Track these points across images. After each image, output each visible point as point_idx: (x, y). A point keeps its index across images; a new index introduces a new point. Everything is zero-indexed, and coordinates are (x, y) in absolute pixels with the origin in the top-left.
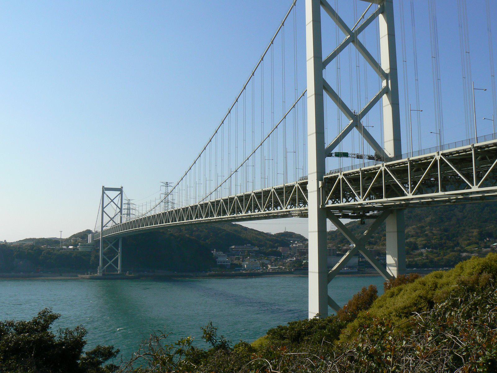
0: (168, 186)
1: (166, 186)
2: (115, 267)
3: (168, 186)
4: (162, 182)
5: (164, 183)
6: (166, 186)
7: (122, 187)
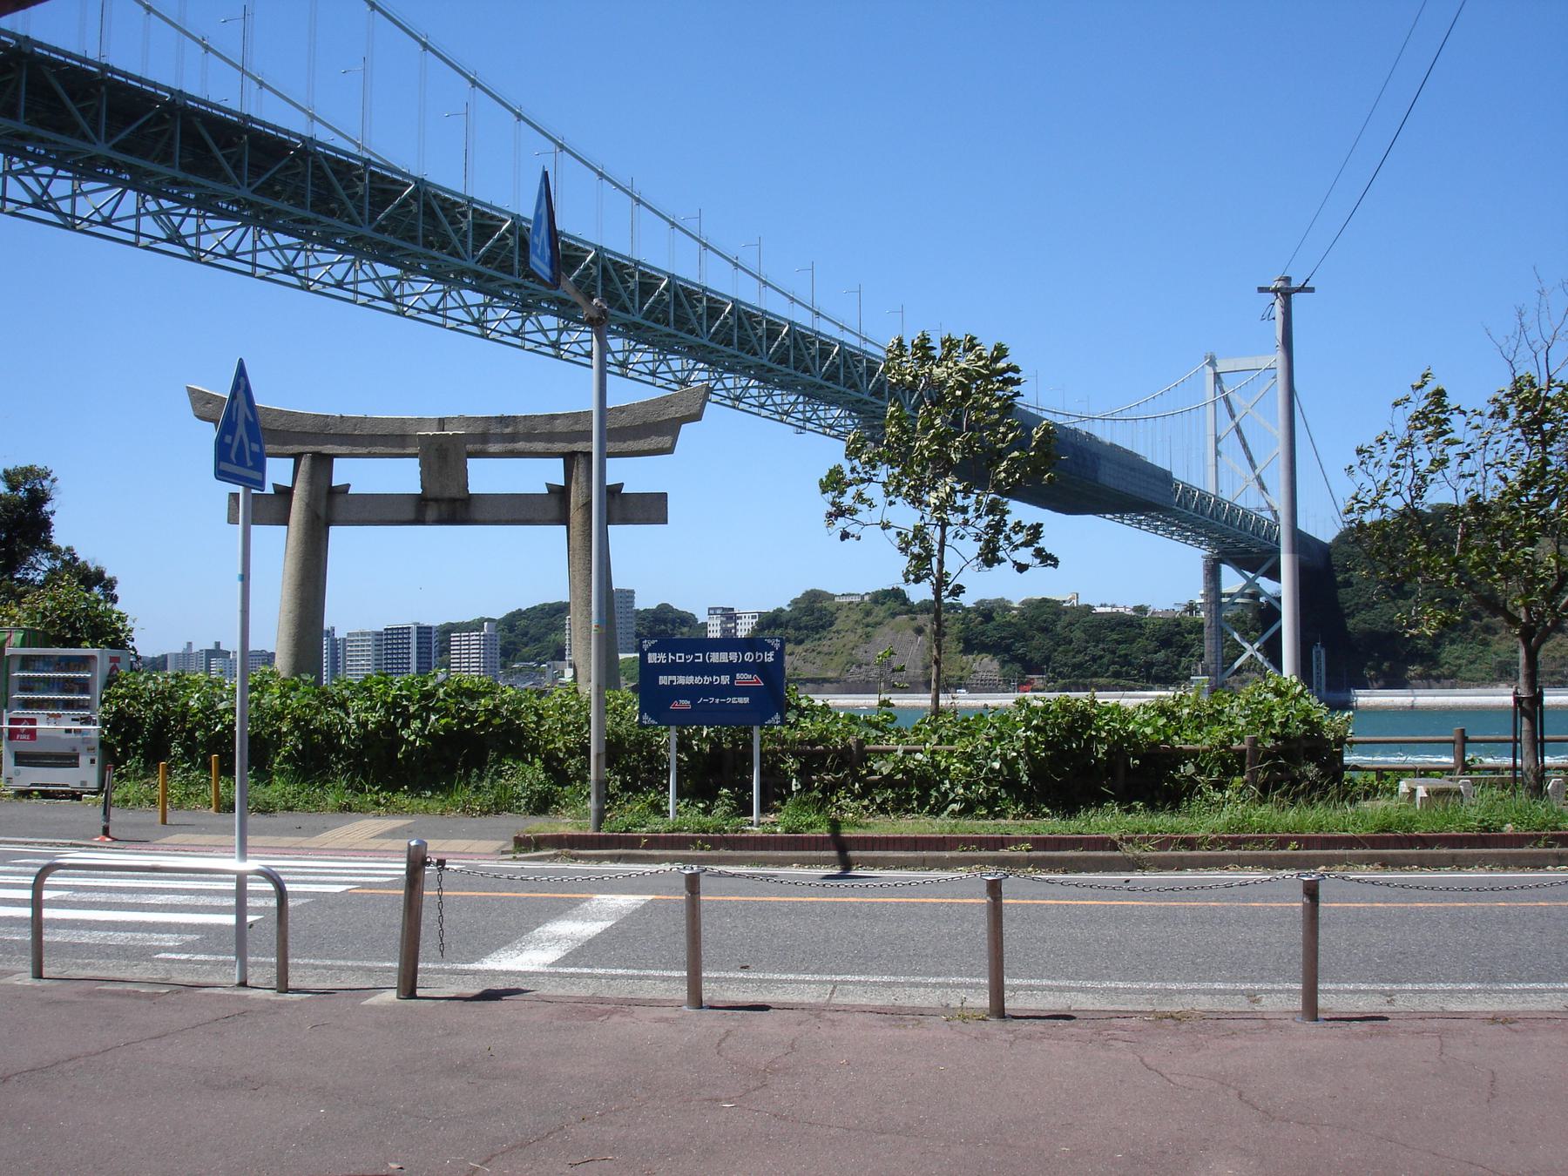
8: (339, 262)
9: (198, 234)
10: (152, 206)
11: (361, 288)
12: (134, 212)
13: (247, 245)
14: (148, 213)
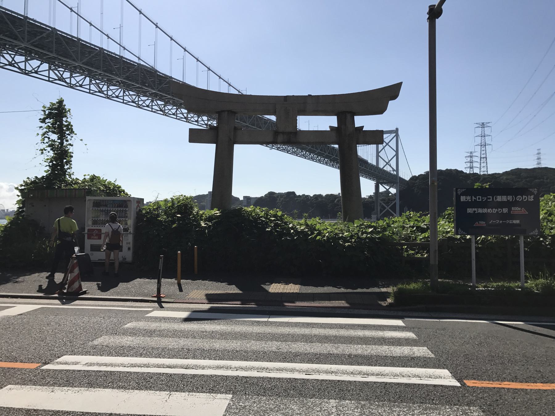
0: (485, 126)
3: (484, 127)
4: (477, 124)
5: (480, 124)
6: (482, 127)
7: (397, 129)
8: (148, 99)
9: (107, 90)
10: (94, 82)
11: (153, 107)
12: (89, 83)
13: (121, 94)
14: (93, 84)
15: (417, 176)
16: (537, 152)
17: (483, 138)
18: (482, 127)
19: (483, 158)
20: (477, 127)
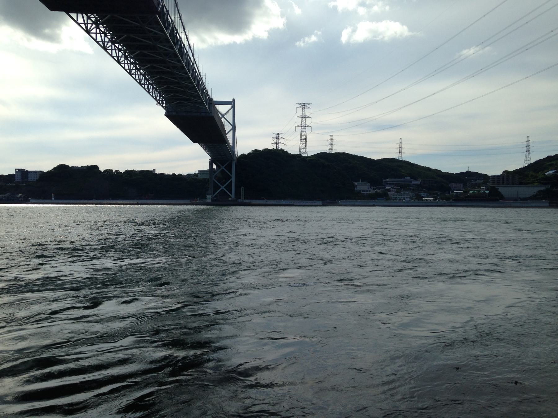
0: (305, 107)
1: (303, 108)
2: (229, 193)
3: (305, 108)
4: (298, 104)
7: (234, 100)
15: (247, 154)
16: (329, 138)
17: (303, 119)
18: (303, 108)
19: (304, 139)
20: (298, 108)
